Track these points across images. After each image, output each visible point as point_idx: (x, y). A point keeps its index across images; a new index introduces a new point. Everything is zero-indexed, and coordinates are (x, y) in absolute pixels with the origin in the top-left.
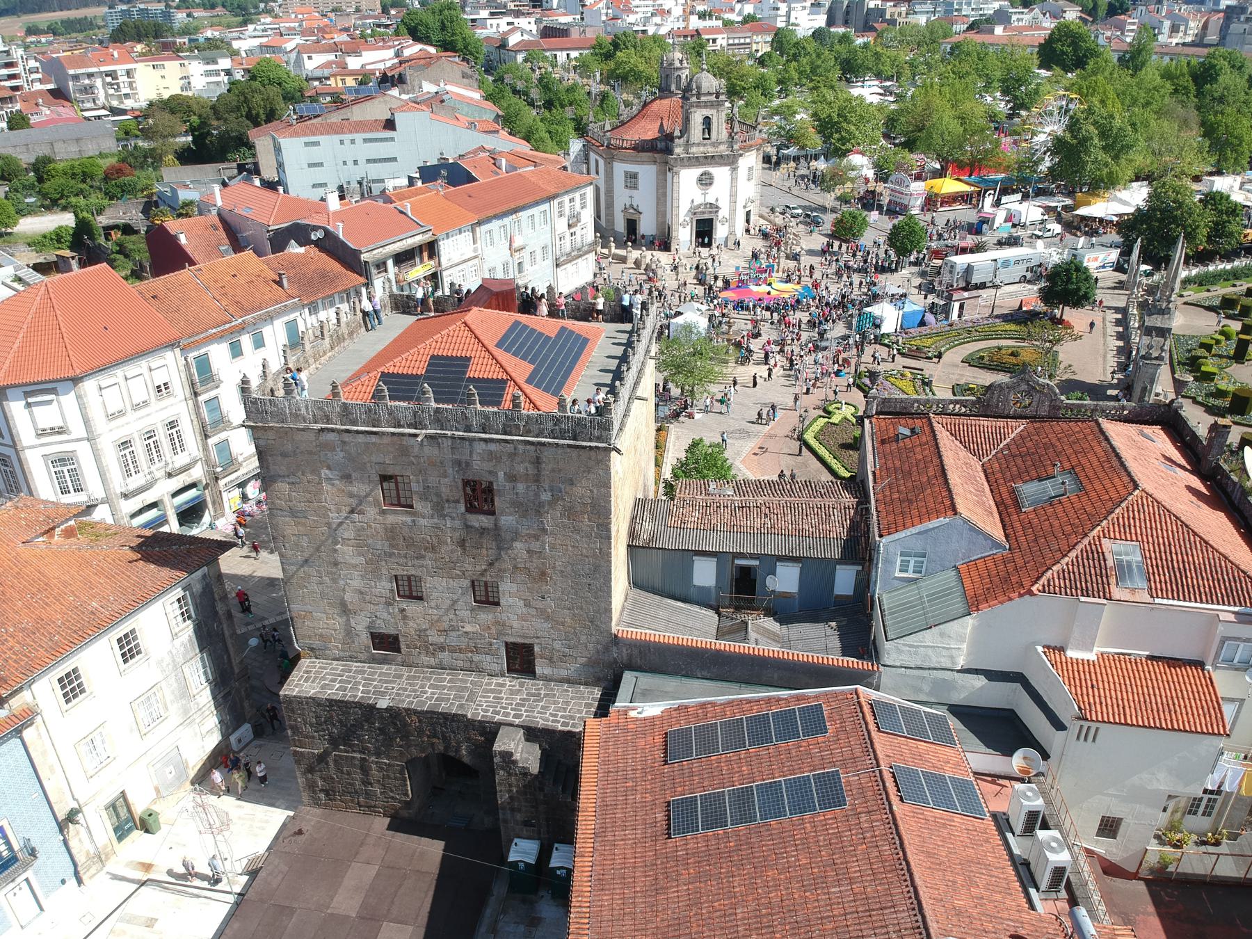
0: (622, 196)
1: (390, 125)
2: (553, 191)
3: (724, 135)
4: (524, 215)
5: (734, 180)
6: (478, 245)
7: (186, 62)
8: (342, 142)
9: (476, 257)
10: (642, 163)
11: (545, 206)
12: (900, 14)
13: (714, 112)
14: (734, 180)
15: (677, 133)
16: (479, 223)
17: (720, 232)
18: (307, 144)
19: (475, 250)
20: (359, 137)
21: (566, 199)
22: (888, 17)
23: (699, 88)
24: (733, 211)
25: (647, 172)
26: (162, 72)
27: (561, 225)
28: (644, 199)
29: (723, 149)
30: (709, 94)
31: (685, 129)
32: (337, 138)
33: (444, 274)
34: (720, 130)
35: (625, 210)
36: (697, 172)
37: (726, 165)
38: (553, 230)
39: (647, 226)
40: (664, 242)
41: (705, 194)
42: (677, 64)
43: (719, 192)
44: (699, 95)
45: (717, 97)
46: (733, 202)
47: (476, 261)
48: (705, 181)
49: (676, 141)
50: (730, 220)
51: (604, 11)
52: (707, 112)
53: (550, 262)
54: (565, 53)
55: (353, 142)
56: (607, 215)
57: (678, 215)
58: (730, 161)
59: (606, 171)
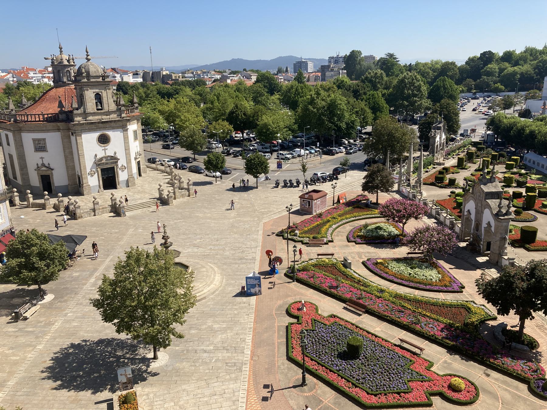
0: (33, 159)
3: (113, 107)
5: (126, 139)
10: (47, 131)
12: (179, 77)
15: (75, 105)
17: (122, 176)
23: (88, 73)
24: (129, 161)
25: (53, 139)
28: (53, 157)
29: (114, 117)
31: (81, 102)
34: (109, 103)
35: (38, 168)
36: (96, 135)
39: (59, 179)
40: (76, 188)
41: (105, 150)
42: (66, 63)
44: (88, 76)
46: (128, 154)
48: (104, 140)
49: (75, 112)
56: (22, 175)
57: (85, 168)
58: (122, 125)
59: (15, 140)
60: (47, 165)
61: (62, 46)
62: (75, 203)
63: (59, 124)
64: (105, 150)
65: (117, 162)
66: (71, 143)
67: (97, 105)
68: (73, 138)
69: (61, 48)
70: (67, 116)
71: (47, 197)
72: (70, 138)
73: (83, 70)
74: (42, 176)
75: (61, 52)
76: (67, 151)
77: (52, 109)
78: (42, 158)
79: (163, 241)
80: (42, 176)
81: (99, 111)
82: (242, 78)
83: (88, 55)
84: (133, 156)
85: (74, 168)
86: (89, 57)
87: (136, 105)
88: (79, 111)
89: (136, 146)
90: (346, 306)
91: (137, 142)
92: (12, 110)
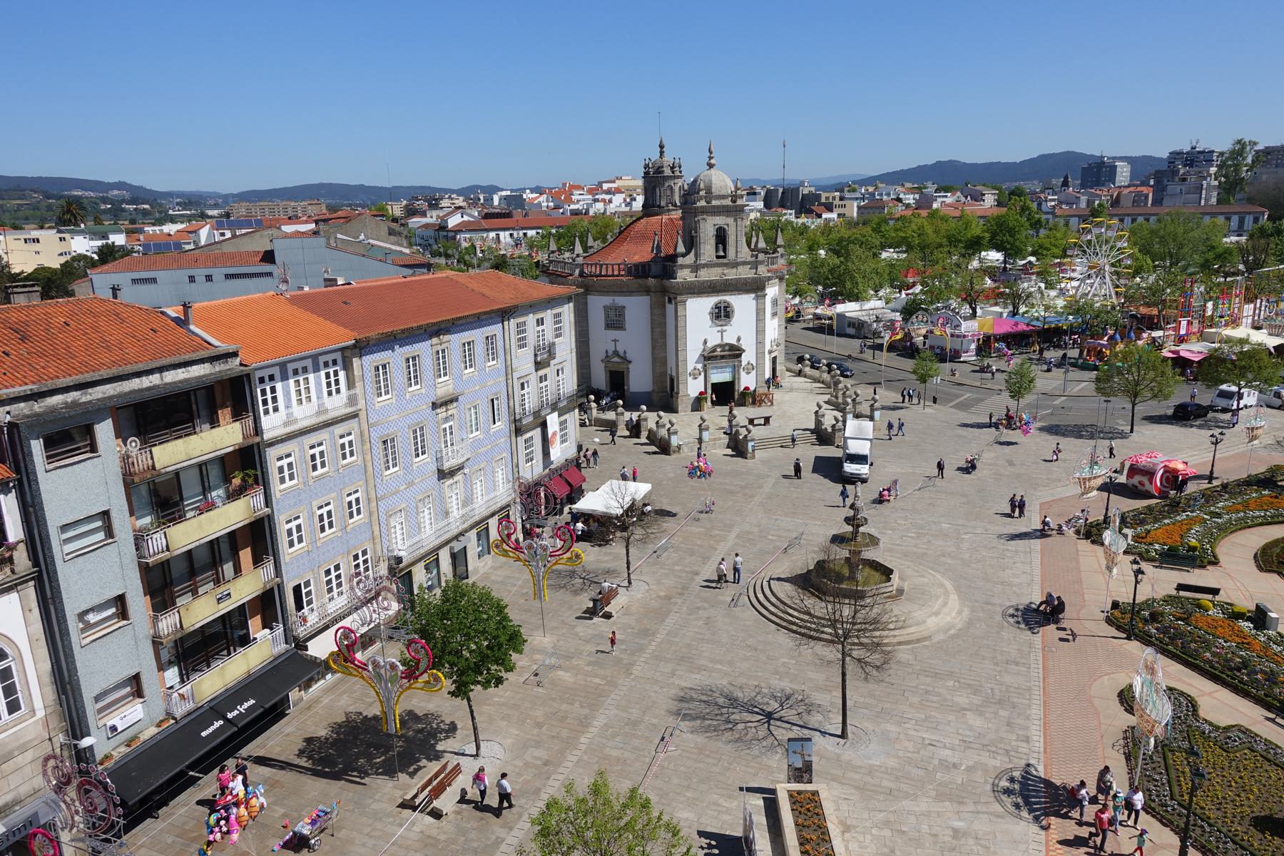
0: (602, 341)
1: (269, 257)
2: (506, 301)
4: (455, 341)
5: (760, 313)
6: (358, 390)
7: (67, 236)
8: (192, 279)
9: (354, 416)
10: (629, 293)
11: (495, 329)
12: (834, 198)
13: (730, 220)
14: (760, 313)
15: (681, 249)
16: (361, 348)
18: (135, 281)
19: (352, 400)
20: (218, 273)
21: (531, 319)
22: (823, 200)
23: (709, 190)
25: (637, 308)
26: (36, 247)
27: (524, 361)
28: (633, 342)
29: (745, 273)
30: (724, 197)
31: (692, 243)
32: (183, 274)
33: (271, 454)
35: (607, 359)
36: (709, 302)
37: (747, 291)
38: (508, 370)
39: (639, 380)
40: (665, 399)
41: (722, 332)
43: (740, 329)
45: (734, 201)
46: (760, 343)
47: (353, 424)
48: (722, 314)
49: (680, 260)
50: (758, 367)
51: (545, 204)
52: (720, 220)
53: (502, 425)
54: (507, 233)
55: (209, 278)
58: (756, 287)
60: (621, 354)
61: (664, 142)
62: (668, 426)
63: (651, 281)
64: (722, 332)
65: (740, 355)
66: (665, 316)
67: (717, 250)
68: (670, 308)
69: (662, 147)
70: (665, 267)
71: (620, 409)
72: (664, 306)
73: (702, 186)
74: (611, 372)
75: (662, 153)
76: (658, 330)
77: (640, 253)
78: (615, 341)
79: (851, 513)
80: (611, 372)
81: (721, 261)
82: (963, 199)
83: (710, 158)
84: (768, 347)
85: (664, 362)
86: (713, 161)
87: (781, 250)
88: (690, 259)
89: (773, 328)
90: (1272, 716)
91: (776, 320)
92: (578, 256)
